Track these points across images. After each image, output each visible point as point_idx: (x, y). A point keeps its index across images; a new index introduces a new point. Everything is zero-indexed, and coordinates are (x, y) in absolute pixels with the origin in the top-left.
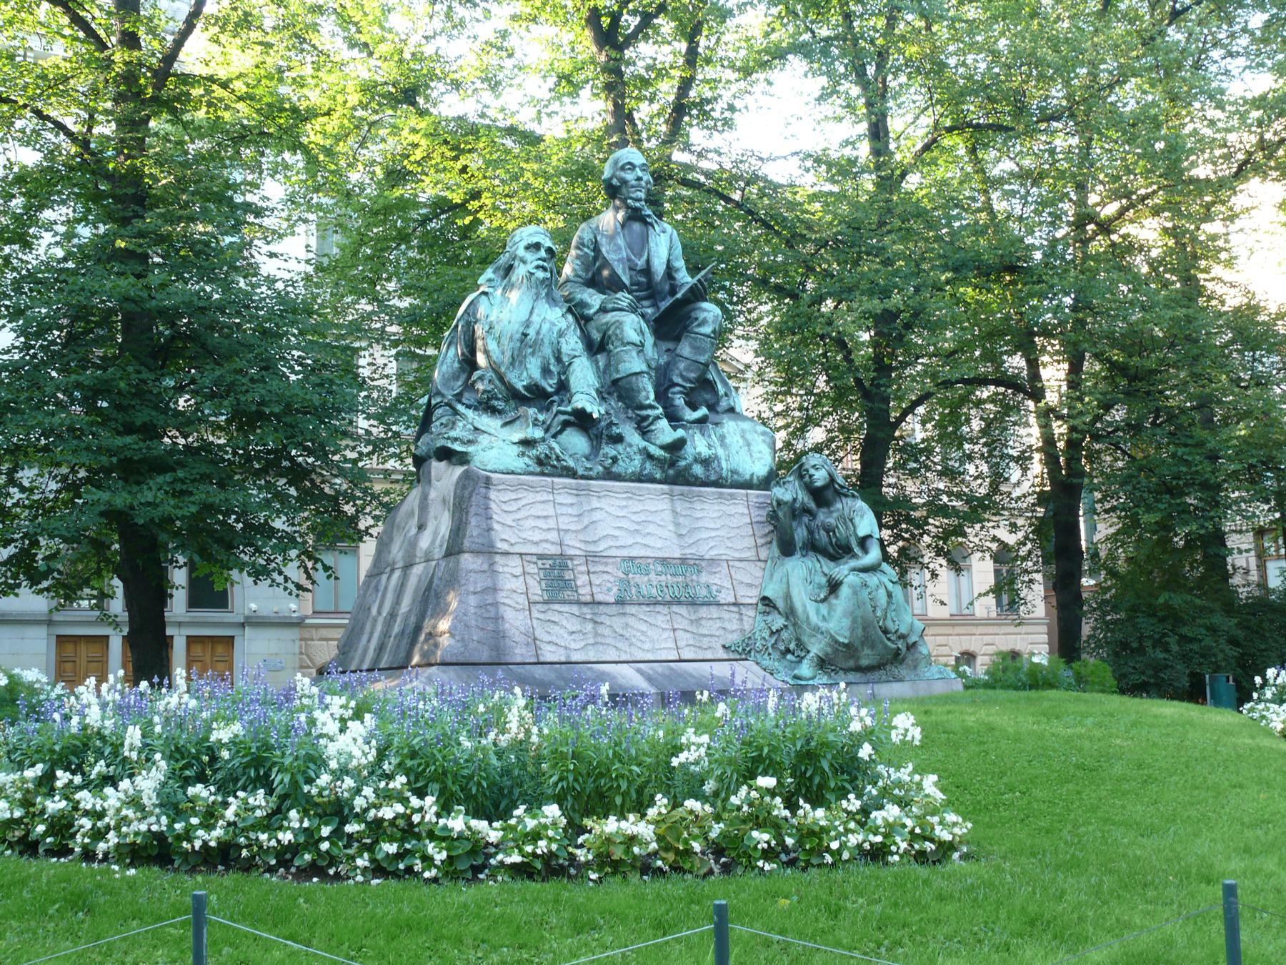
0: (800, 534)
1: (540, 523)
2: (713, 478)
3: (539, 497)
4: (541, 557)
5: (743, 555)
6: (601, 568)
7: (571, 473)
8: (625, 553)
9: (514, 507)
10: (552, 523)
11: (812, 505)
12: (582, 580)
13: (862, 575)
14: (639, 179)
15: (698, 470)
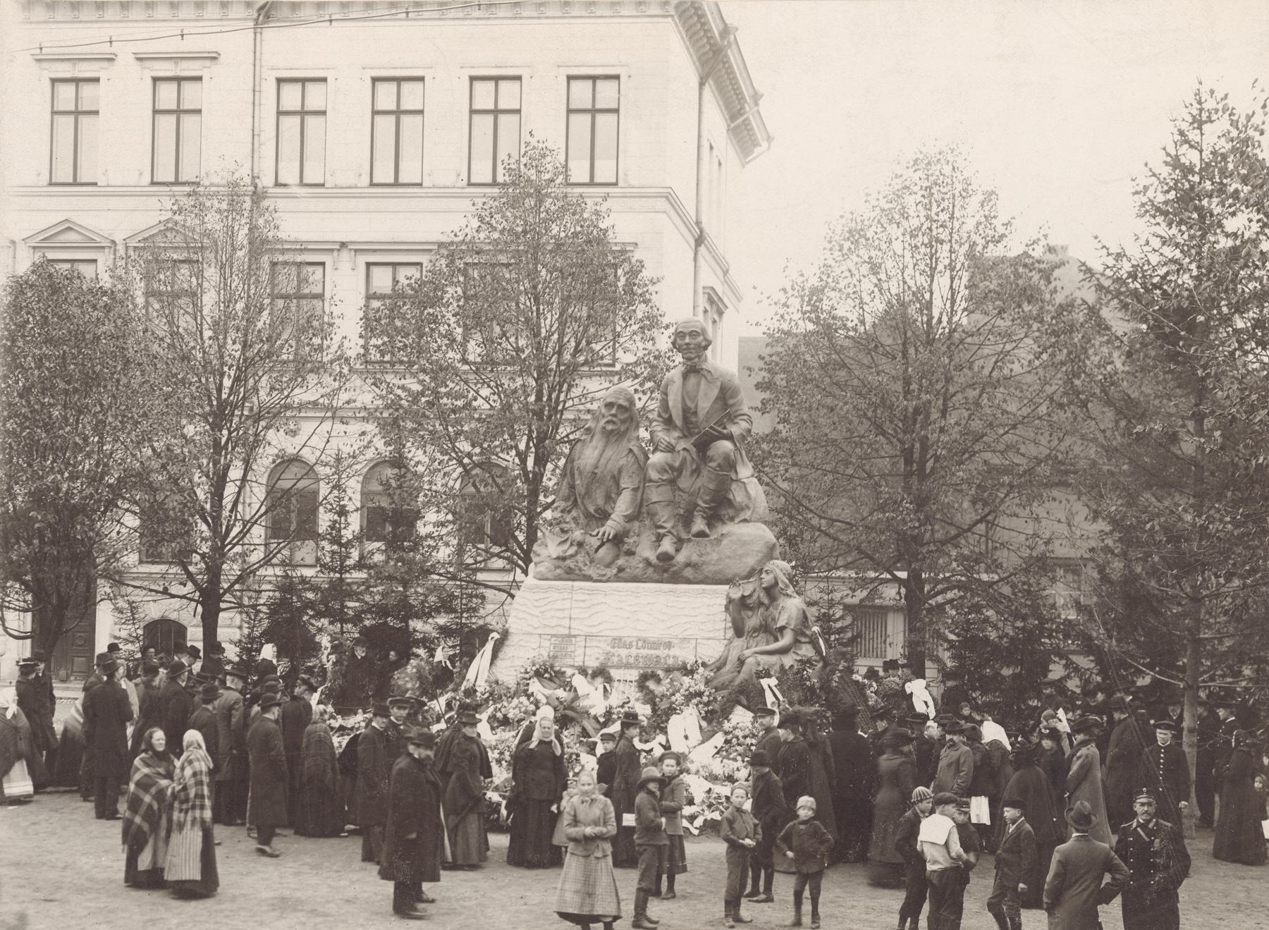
0: (753, 621)
1: (560, 614)
2: (700, 577)
3: (561, 596)
4: (554, 636)
5: (711, 635)
6: (595, 644)
7: (588, 578)
8: (616, 634)
9: (543, 602)
10: (566, 614)
11: (766, 601)
12: (580, 651)
13: (760, 657)
14: (687, 344)
15: (688, 572)
